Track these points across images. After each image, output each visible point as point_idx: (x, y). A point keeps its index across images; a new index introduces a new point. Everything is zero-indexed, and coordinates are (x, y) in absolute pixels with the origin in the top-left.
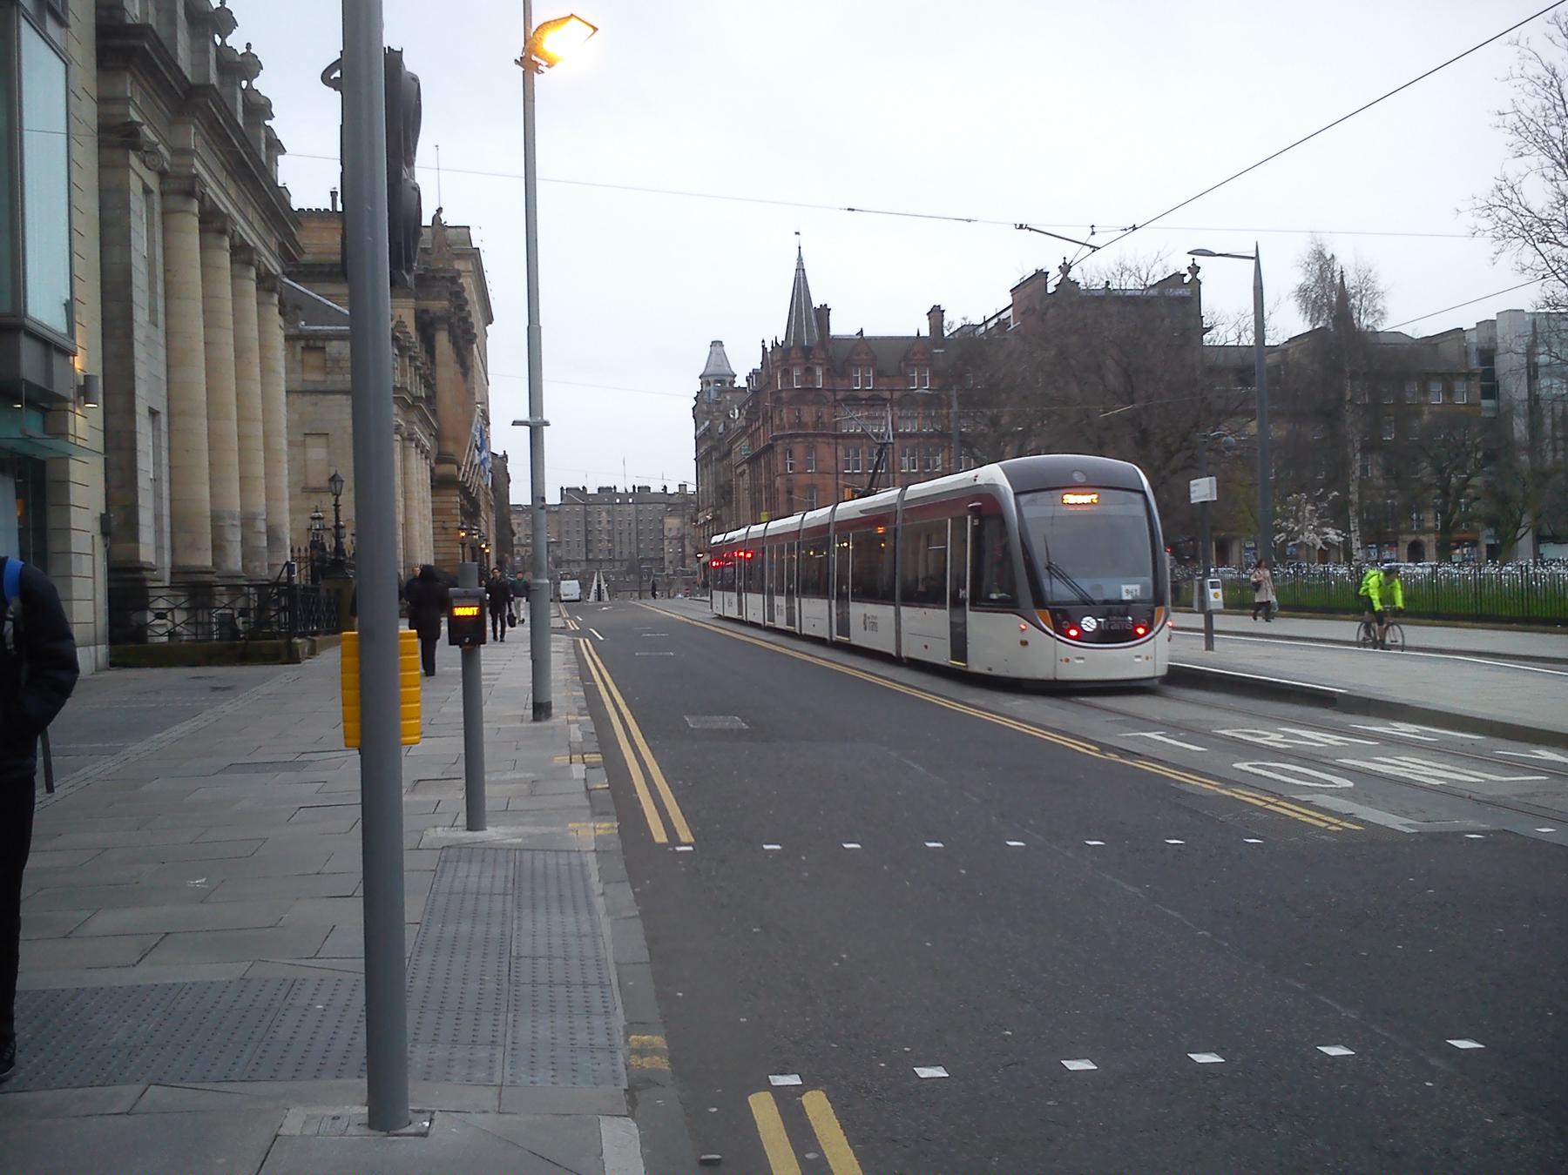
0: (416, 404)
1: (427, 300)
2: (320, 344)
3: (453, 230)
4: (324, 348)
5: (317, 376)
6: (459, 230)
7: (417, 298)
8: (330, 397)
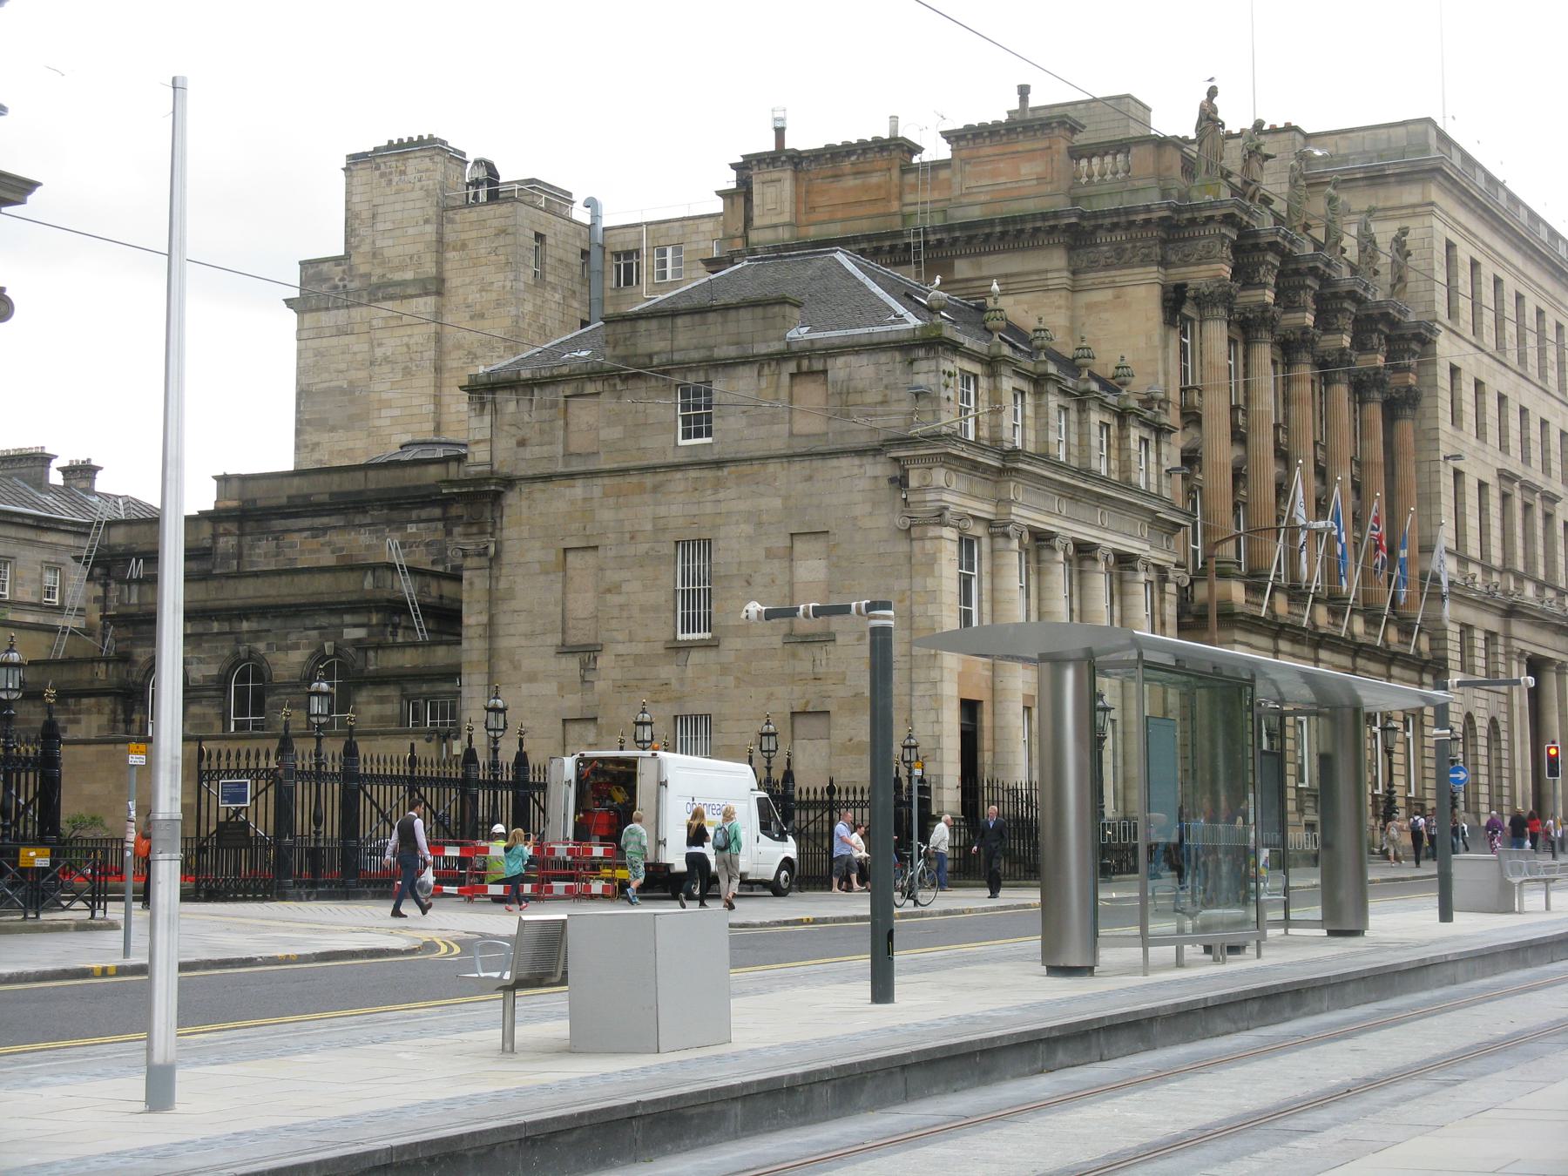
0: (1009, 465)
1: (1186, 264)
2: (818, 365)
3: (1401, 131)
4: (825, 372)
5: (809, 425)
6: (1411, 127)
7: (1164, 263)
8: (834, 462)
